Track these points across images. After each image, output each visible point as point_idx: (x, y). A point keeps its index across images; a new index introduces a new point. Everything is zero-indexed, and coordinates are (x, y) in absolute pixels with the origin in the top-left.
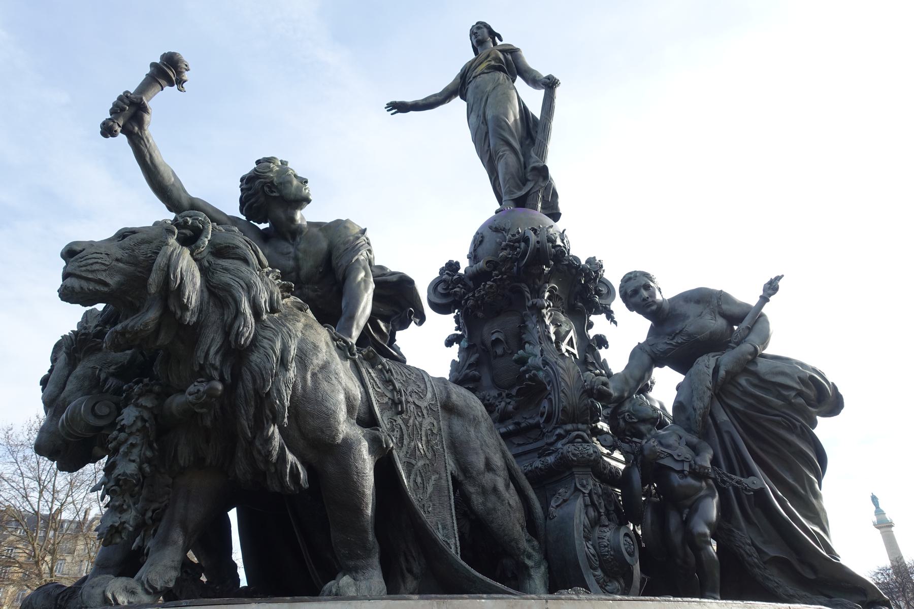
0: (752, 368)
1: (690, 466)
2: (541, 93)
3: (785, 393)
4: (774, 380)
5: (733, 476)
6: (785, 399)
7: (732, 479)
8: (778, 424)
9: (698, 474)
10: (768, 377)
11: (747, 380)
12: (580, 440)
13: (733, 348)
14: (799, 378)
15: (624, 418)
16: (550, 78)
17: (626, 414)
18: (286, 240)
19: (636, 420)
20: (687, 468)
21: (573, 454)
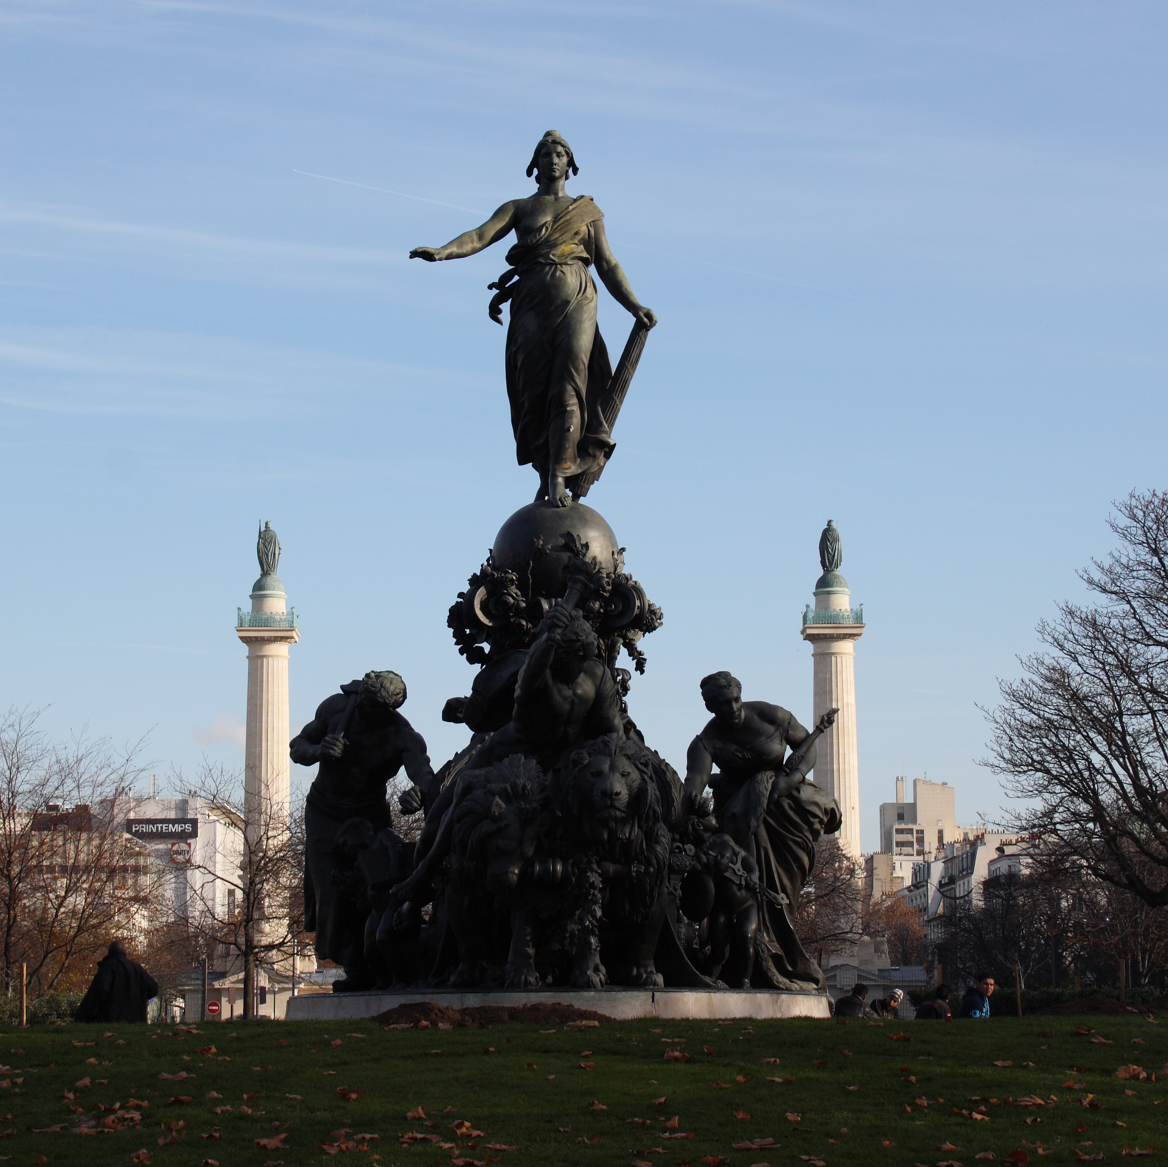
0: (795, 793)
1: (746, 880)
2: (630, 320)
3: (812, 819)
4: (808, 808)
5: (772, 893)
6: (810, 825)
7: (770, 895)
8: (797, 844)
9: (749, 888)
10: (804, 805)
11: (789, 804)
12: (677, 850)
13: (787, 775)
14: (825, 809)
15: (693, 825)
16: (649, 316)
17: (696, 820)
18: (567, 684)
19: (702, 828)
20: (743, 883)
21: (676, 865)
